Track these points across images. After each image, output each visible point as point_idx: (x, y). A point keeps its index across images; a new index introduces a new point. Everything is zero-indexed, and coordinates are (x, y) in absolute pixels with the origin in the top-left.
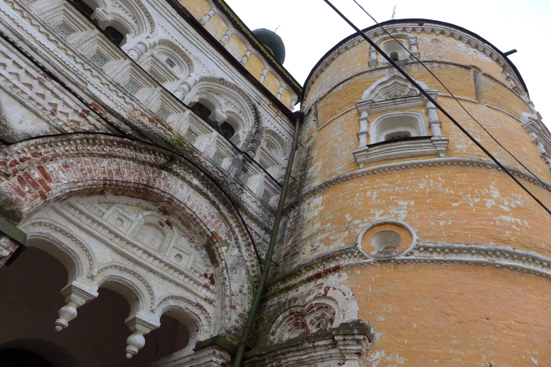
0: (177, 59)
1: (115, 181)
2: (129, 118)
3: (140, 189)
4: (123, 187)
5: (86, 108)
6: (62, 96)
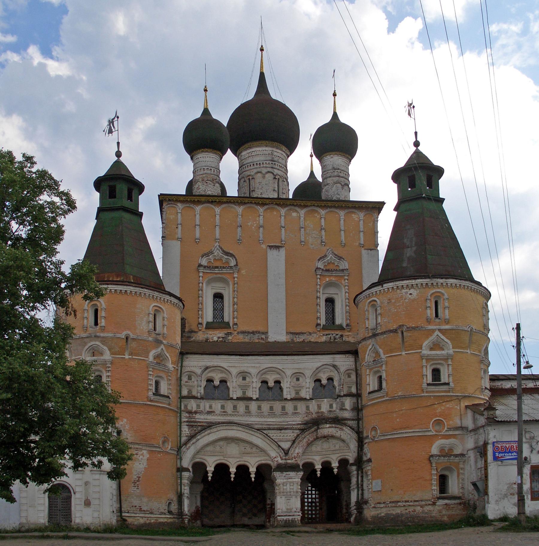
6: (286, 432)
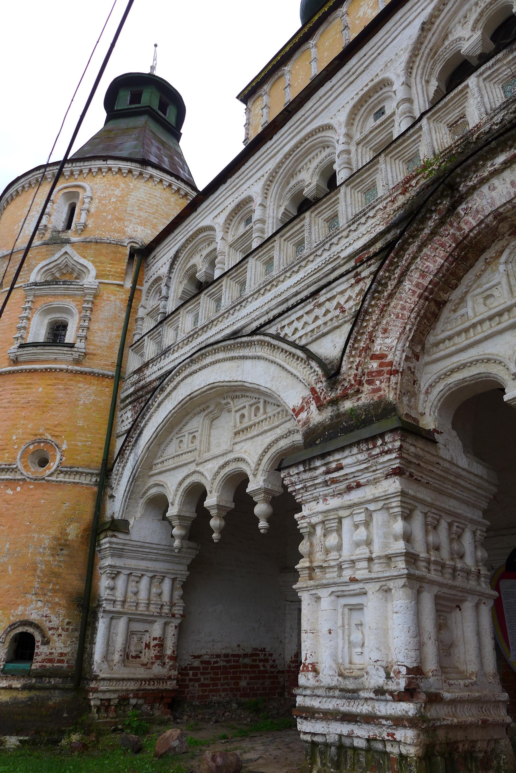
0: (377, 101)
1: (429, 284)
2: (387, 223)
3: (459, 255)
4: (443, 277)
5: (352, 274)
6: (334, 292)
